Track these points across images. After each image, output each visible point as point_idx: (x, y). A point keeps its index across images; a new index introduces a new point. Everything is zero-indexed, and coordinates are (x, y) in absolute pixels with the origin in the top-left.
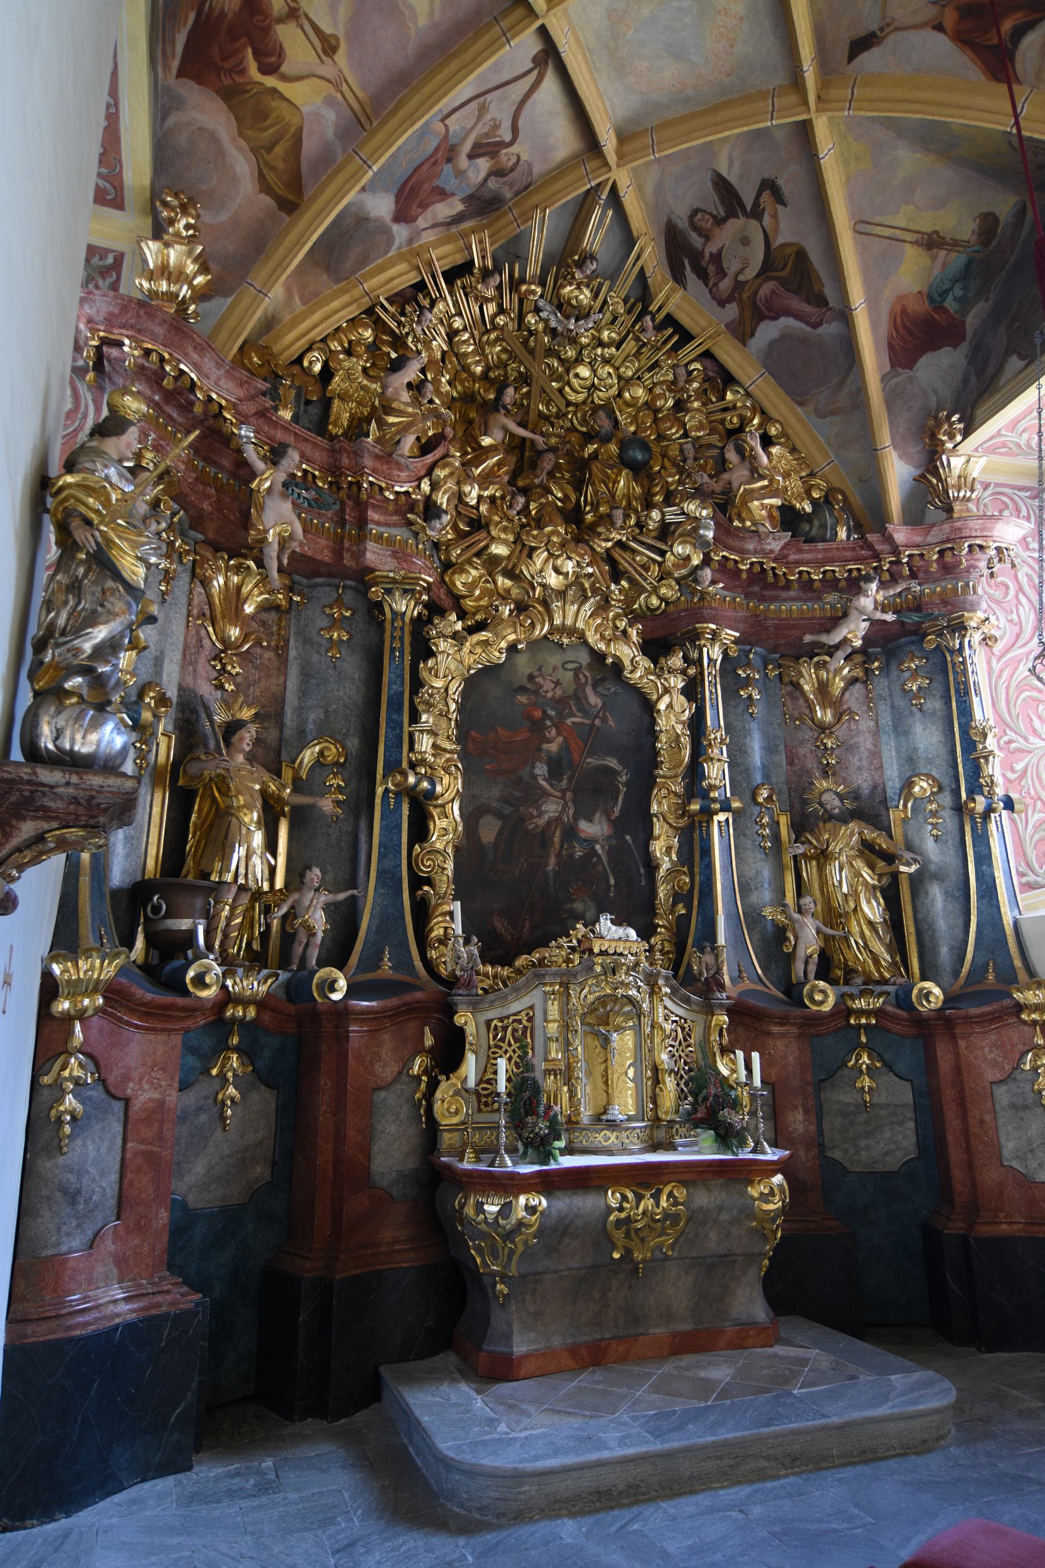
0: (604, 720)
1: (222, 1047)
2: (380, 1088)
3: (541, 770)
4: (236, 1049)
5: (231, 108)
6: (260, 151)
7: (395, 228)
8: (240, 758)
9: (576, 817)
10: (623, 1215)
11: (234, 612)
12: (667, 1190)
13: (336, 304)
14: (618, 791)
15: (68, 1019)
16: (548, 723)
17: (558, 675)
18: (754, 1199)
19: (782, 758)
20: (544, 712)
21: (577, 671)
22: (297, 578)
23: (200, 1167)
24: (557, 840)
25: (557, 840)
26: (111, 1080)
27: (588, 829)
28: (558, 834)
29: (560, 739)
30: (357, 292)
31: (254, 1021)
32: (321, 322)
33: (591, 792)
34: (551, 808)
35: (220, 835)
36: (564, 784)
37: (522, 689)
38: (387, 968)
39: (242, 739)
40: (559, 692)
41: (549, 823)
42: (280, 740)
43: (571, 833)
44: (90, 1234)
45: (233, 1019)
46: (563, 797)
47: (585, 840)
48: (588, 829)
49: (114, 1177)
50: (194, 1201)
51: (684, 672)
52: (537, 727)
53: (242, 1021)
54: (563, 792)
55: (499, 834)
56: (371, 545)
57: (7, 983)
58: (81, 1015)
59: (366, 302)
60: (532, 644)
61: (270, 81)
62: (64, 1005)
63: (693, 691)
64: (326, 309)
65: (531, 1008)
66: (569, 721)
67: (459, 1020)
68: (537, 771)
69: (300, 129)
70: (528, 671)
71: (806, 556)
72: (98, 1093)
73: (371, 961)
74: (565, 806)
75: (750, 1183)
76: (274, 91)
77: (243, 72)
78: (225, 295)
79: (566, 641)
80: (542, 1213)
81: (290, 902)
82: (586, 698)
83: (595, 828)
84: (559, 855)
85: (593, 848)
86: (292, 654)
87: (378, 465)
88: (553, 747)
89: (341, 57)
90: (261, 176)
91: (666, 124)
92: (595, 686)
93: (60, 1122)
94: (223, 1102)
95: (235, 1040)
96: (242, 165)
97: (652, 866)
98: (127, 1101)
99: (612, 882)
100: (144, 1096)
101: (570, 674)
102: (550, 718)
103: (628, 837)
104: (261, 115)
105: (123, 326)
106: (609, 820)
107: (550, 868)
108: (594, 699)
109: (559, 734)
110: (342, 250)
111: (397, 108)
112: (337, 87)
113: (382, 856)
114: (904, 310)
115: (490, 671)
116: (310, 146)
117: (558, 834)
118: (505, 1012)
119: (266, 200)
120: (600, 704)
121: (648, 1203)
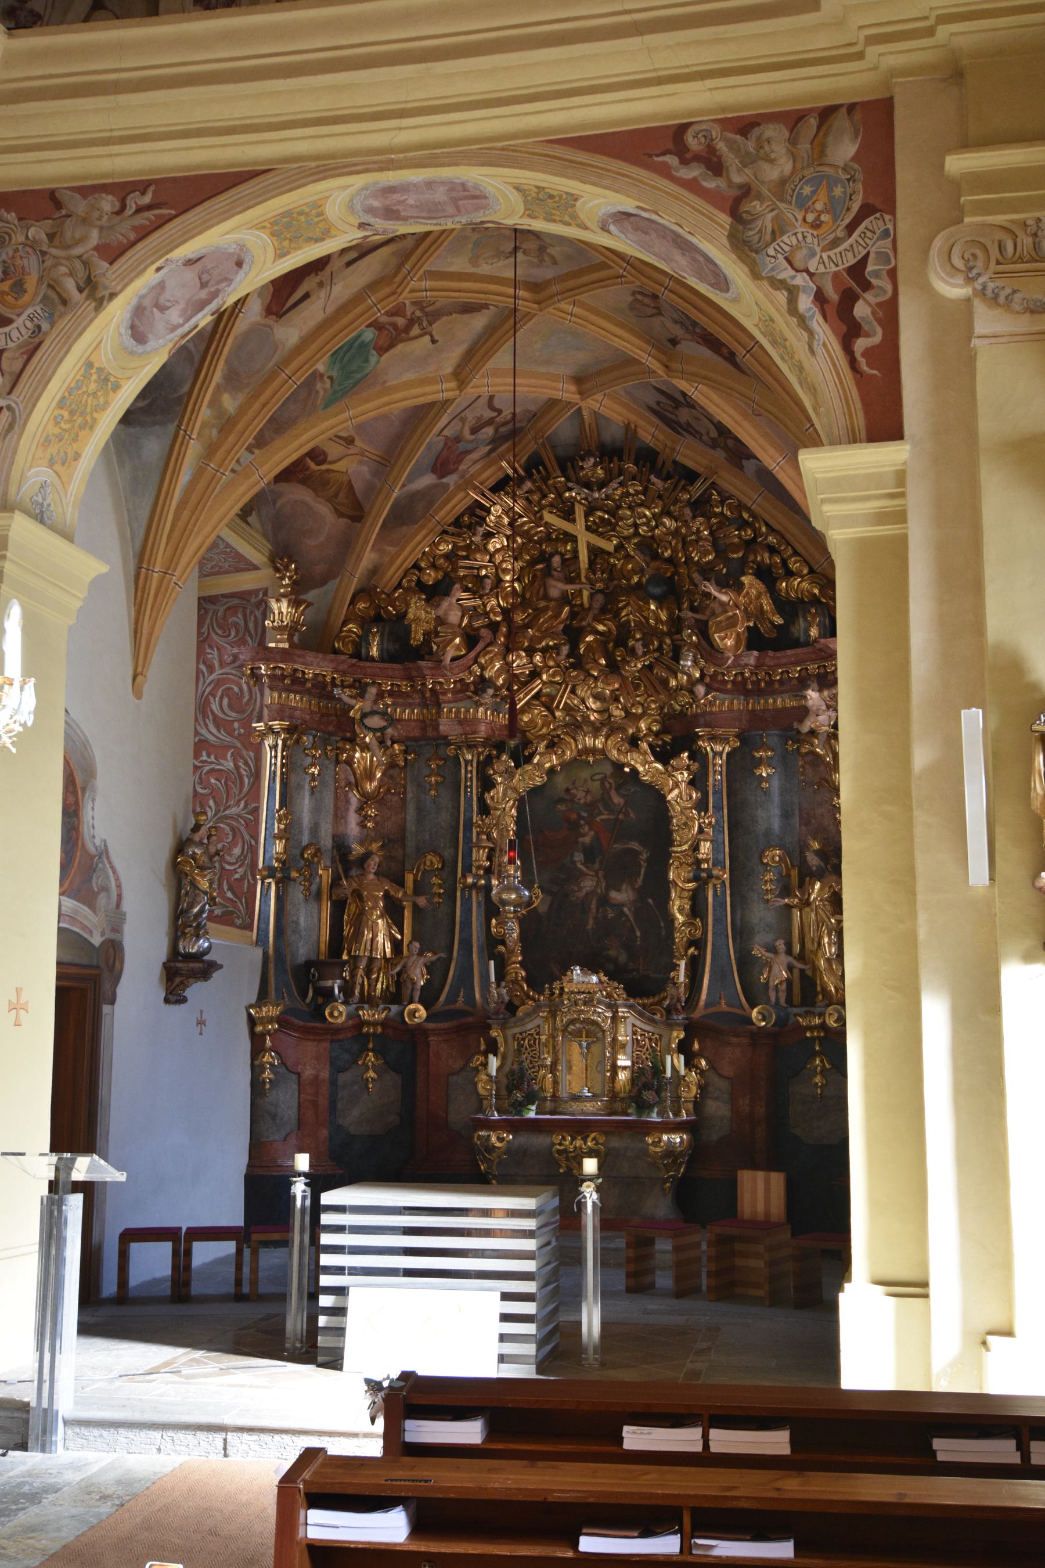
0: (627, 814)
2: (452, 1074)
3: (579, 857)
4: (372, 1050)
5: (308, 486)
6: (331, 500)
7: (444, 480)
8: (371, 876)
9: (608, 888)
10: (562, 1148)
12: (593, 1135)
13: (419, 538)
14: (640, 866)
15: (263, 1035)
16: (582, 822)
17: (587, 786)
18: (648, 1144)
19: (796, 821)
20: (579, 815)
21: (603, 780)
22: (408, 743)
23: (355, 1113)
24: (593, 906)
25: (593, 906)
26: (289, 1064)
27: (616, 896)
28: (594, 902)
29: (592, 833)
30: (431, 525)
31: (381, 1034)
32: (410, 554)
33: (619, 869)
34: (588, 884)
36: (597, 866)
37: (561, 800)
38: (460, 1003)
39: (369, 865)
40: (589, 798)
41: (587, 894)
42: (404, 855)
43: (604, 901)
44: (284, 1134)
45: (368, 1034)
46: (597, 875)
47: (615, 905)
48: (616, 896)
49: (295, 1110)
50: (352, 1130)
51: (688, 768)
52: (574, 827)
54: (597, 872)
55: (551, 906)
57: (201, 1023)
58: (269, 1033)
59: (439, 528)
60: (565, 765)
61: (324, 467)
64: (413, 543)
65: (539, 1026)
66: (598, 819)
67: (494, 1034)
68: (576, 858)
69: (350, 481)
70: (565, 786)
71: (784, 661)
72: (283, 1070)
73: (452, 998)
74: (598, 882)
75: (648, 1134)
76: (328, 471)
77: (308, 469)
78: (334, 578)
79: (591, 759)
80: (508, 1142)
81: (402, 963)
82: (610, 799)
83: (622, 896)
84: (596, 918)
85: (622, 910)
86: (410, 795)
87: (434, 672)
88: (587, 840)
89: (358, 442)
90: (336, 510)
91: (600, 373)
92: (617, 789)
93: (264, 1082)
94: (367, 1080)
95: (371, 1046)
96: (324, 510)
97: (672, 920)
98: (299, 1075)
99: (638, 934)
100: (308, 1072)
101: (598, 783)
102: (583, 818)
103: (650, 901)
104: (325, 483)
105: (259, 660)
106: (634, 889)
107: (590, 927)
108: (617, 800)
109: (591, 829)
110: (405, 515)
111: (401, 453)
112: (362, 455)
113: (462, 929)
115: (534, 791)
116: (358, 486)
117: (594, 902)
118: (524, 1029)
119: (343, 521)
120: (622, 801)
121: (578, 1143)
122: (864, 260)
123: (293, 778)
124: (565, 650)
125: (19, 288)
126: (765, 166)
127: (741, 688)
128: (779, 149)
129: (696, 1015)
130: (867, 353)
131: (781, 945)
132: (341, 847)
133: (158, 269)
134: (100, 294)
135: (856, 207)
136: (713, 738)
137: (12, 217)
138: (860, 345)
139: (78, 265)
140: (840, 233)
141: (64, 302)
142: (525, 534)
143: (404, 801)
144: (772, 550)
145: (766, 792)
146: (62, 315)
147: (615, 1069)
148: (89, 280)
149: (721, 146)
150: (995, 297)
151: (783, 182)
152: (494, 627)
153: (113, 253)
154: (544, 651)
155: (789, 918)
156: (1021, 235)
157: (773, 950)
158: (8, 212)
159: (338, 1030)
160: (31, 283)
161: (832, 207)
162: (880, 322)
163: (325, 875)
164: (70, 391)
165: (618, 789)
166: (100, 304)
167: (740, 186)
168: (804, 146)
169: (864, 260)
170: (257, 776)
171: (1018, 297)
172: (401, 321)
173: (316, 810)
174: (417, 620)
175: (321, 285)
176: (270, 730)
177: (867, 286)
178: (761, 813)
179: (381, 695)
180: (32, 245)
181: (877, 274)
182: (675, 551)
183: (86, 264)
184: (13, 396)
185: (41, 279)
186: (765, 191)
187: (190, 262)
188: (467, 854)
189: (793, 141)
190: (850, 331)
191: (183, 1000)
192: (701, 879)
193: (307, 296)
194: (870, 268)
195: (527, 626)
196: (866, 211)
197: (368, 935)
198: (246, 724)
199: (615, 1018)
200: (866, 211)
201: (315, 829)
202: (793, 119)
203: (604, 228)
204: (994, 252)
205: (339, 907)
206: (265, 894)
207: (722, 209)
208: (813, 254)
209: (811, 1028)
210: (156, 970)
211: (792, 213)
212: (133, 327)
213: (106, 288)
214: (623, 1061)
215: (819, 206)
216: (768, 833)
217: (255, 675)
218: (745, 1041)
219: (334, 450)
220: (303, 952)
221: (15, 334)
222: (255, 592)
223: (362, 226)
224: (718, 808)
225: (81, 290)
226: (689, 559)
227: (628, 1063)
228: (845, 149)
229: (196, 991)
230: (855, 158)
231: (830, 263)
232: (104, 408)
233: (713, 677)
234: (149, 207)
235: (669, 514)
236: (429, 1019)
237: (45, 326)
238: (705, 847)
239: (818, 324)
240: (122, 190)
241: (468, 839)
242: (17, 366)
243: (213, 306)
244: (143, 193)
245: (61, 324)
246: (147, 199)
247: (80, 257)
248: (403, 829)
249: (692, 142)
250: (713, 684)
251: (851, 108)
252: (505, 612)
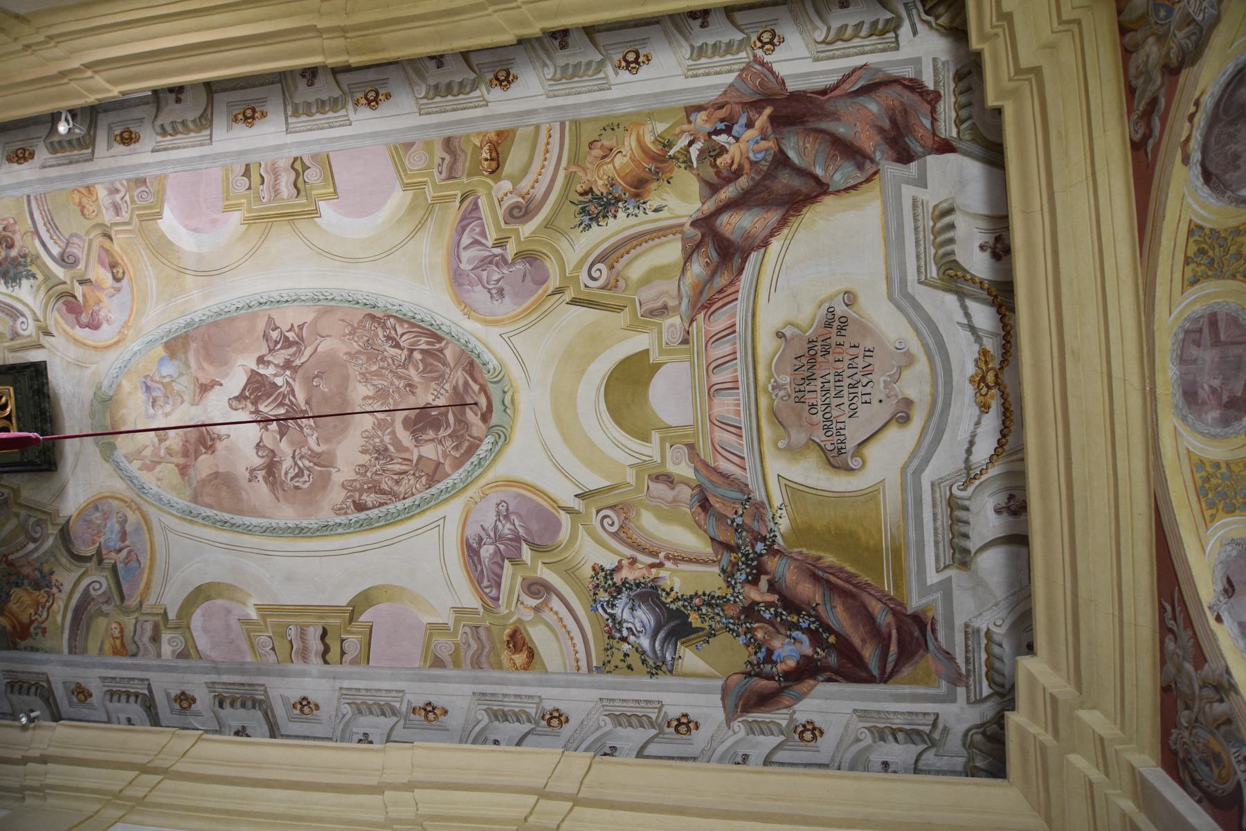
125: (1217, 757)
133: (1219, 619)
134: (1226, 685)
139: (1206, 692)
141: (1229, 721)
153: (1200, 659)
158: (1171, 735)
166: (1233, 687)
167: (1163, 75)
168: (1139, 36)
186: (1164, 52)
187: (1230, 589)
207: (1177, 81)
213: (1221, 675)
240: (1164, 630)
244: (1165, 611)
246: (1169, 608)
247: (1201, 688)
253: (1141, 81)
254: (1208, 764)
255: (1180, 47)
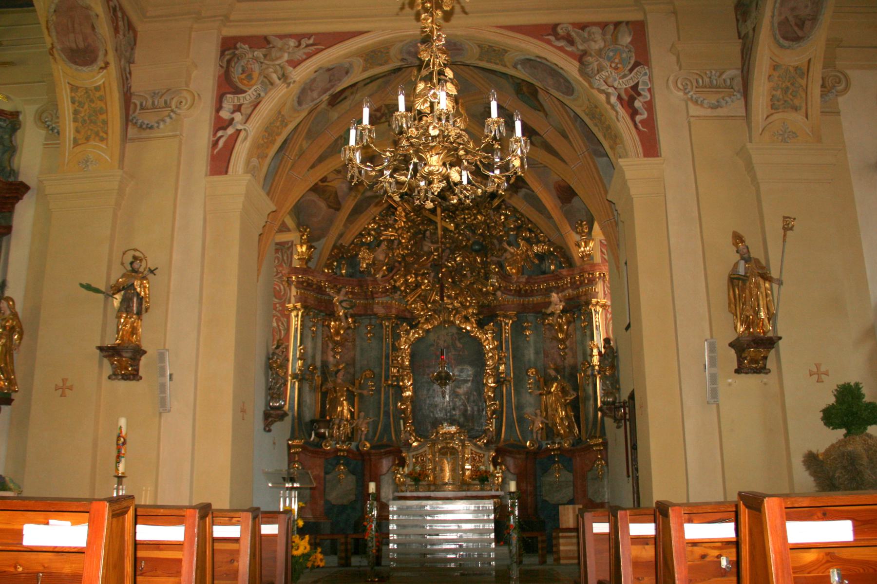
1: (338, 464)
4: (343, 464)
11: (337, 333)
19: (542, 355)
21: (452, 335)
35: (335, 403)
50: (334, 502)
53: (343, 456)
56: (376, 306)
57: (274, 443)
62: (292, 451)
63: (498, 336)
69: (336, 193)
96: (322, 205)
108: (459, 345)
113: (385, 407)
114: (559, 186)
116: (340, 194)
122: (638, 83)
123: (305, 332)
124: (432, 274)
125: (250, 77)
126: (593, 44)
127: (518, 293)
128: (598, 37)
129: (501, 444)
130: (642, 122)
131: (538, 411)
132: (325, 364)
135: (632, 62)
136: (506, 317)
137: (246, 47)
138: (638, 118)
139: (278, 67)
140: (626, 72)
141: (272, 84)
142: (412, 221)
143: (354, 345)
144: (531, 231)
145: (528, 342)
146: (270, 90)
147: (464, 470)
148: (283, 75)
149: (573, 34)
150: (697, 101)
151: (600, 50)
152: (400, 263)
154: (424, 274)
155: (540, 401)
156: (705, 77)
157: (536, 415)
159: (327, 453)
160: (255, 75)
161: (622, 61)
162: (646, 109)
163: (318, 380)
164: (270, 124)
165: (460, 339)
167: (582, 51)
168: (609, 37)
169: (638, 83)
170: (288, 329)
171: (706, 102)
172: (379, 114)
173: (314, 348)
174: (364, 258)
175: (352, 93)
176: (295, 307)
177: (639, 94)
178: (526, 352)
179: (347, 293)
180: (256, 59)
181: (643, 90)
182: (483, 230)
183: (282, 68)
184: (247, 125)
185: (260, 74)
186: (593, 53)
188: (388, 370)
189: (604, 34)
190: (634, 113)
191: (270, 431)
192: (499, 382)
193: (345, 98)
194: (640, 87)
195: (413, 263)
196: (636, 64)
197: (339, 409)
198: (283, 305)
199: (464, 446)
200: (636, 64)
201: (314, 357)
202: (603, 26)
203: (515, 67)
204: (695, 84)
205: (324, 395)
206: (293, 387)
207: (575, 59)
208: (615, 80)
209: (553, 450)
210: (262, 413)
211: (606, 64)
212: (299, 98)
214: (468, 466)
215: (617, 61)
216: (529, 361)
217: (289, 282)
218: (523, 456)
219: (331, 177)
220: (308, 416)
221: (248, 97)
222: (287, 243)
223: (403, 60)
224: (507, 349)
225: (280, 79)
226: (491, 234)
227: (470, 467)
228: (626, 39)
229: (277, 426)
230: (631, 43)
231: (624, 84)
232: (279, 134)
233: (505, 288)
234: (312, 45)
235: (481, 214)
236: (372, 448)
237: (262, 94)
238: (502, 368)
239: (619, 107)
241: (387, 364)
242: (249, 112)
243: (330, 92)
244: (309, 39)
245: (269, 94)
246: (311, 41)
247: (279, 65)
248: (354, 359)
249: (559, 30)
250: (506, 291)
251: (627, 23)
252: (403, 257)
253: (586, 35)
254: (243, 72)
255: (591, 63)
